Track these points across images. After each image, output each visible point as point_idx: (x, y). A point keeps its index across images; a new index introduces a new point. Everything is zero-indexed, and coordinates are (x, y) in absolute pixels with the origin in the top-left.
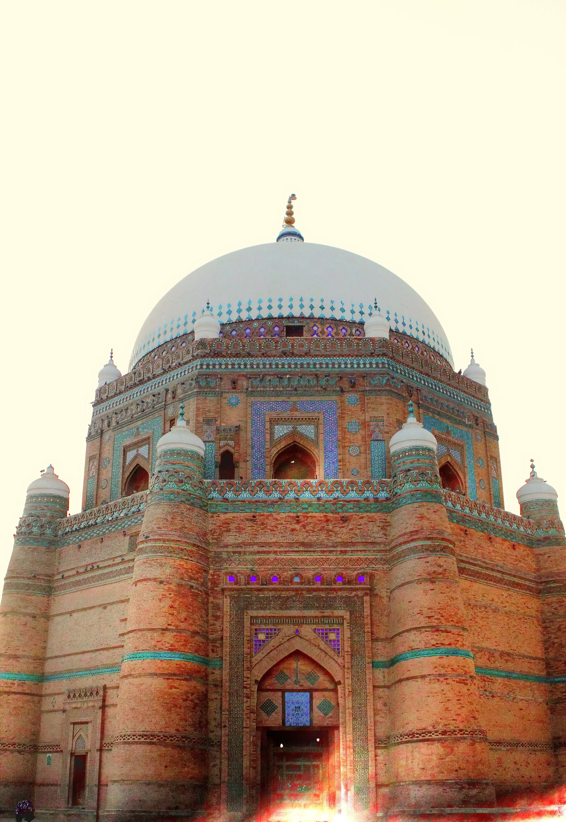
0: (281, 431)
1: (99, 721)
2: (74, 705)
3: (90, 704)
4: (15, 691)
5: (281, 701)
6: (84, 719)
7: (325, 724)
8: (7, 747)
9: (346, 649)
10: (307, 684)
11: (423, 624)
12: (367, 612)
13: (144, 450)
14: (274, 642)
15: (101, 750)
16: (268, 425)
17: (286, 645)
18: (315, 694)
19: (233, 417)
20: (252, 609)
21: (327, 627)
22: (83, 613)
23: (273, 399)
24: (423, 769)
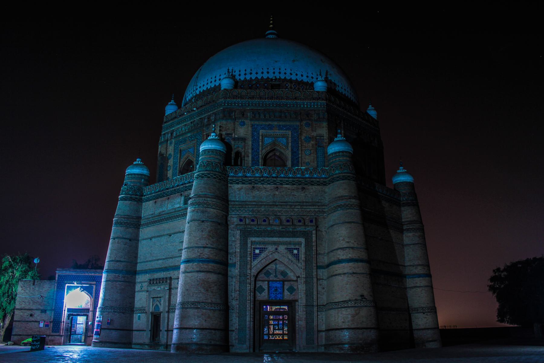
0: (268, 141)
1: (167, 296)
5: (267, 286)
6: (159, 296)
7: (291, 299)
9: (303, 259)
10: (281, 277)
11: (345, 246)
12: (314, 239)
14: (263, 255)
15: (168, 312)
16: (261, 138)
17: (271, 256)
18: (286, 283)
19: (242, 131)
20: (252, 237)
21: (293, 247)
22: (159, 238)
23: (264, 123)
24: (343, 322)
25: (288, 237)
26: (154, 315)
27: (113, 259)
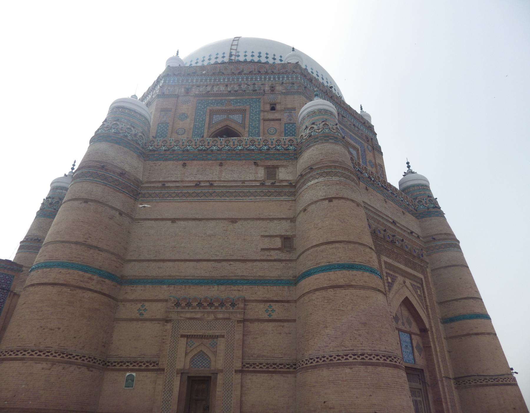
1: (238, 336)
2: (188, 315)
3: (220, 316)
4: (92, 288)
6: (210, 332)
8: (73, 360)
13: (237, 118)
14: (395, 287)
21: (415, 284)
22: (198, 222)
25: (411, 268)
26: (189, 377)
27: (81, 240)
